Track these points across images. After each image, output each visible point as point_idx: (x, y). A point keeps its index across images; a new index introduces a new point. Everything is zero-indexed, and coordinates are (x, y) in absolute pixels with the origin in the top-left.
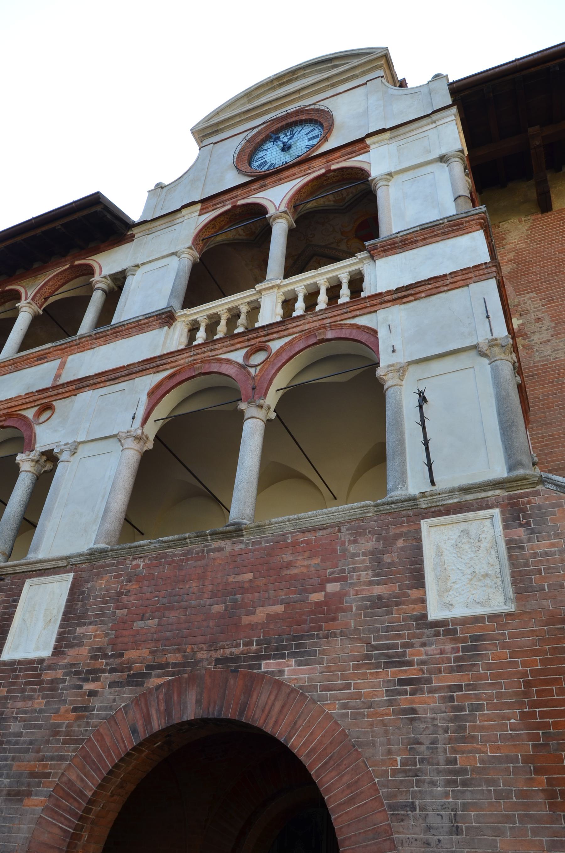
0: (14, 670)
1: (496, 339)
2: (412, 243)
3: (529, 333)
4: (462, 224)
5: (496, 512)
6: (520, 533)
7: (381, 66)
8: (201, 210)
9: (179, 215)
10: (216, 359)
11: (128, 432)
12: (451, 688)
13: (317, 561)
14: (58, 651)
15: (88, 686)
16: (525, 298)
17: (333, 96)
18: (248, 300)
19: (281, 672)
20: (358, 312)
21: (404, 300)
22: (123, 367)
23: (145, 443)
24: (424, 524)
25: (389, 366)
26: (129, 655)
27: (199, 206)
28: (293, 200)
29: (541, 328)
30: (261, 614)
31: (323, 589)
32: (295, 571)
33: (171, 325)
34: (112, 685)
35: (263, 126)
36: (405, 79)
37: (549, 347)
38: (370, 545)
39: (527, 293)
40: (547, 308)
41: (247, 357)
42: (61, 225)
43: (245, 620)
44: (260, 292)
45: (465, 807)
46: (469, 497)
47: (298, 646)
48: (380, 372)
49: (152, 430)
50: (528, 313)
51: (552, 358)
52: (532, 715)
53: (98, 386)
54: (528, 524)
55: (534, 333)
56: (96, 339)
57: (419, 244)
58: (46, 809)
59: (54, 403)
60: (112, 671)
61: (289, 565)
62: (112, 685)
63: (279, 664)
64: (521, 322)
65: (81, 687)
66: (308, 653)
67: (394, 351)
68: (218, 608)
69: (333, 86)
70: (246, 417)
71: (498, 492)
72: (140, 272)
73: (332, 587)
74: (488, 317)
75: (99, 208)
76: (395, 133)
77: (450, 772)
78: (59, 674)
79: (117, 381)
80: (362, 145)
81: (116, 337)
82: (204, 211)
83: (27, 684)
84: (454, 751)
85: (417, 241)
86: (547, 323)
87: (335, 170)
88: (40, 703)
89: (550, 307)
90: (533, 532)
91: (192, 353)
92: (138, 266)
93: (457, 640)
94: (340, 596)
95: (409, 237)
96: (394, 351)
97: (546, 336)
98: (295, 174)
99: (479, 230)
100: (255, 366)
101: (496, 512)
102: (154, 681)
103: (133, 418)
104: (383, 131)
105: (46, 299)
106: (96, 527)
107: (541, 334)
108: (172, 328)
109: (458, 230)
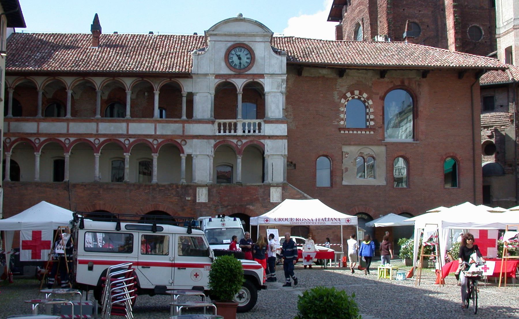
5: (281, 188)
6: (284, 192)
10: (230, 141)
13: (254, 191)
14: (209, 201)
24: (271, 188)
30: (246, 199)
38: (263, 190)
43: (243, 199)
68: (239, 197)
73: (257, 196)
78: (210, 205)
88: (208, 210)
100: (239, 146)
101: (281, 188)
102: (229, 207)
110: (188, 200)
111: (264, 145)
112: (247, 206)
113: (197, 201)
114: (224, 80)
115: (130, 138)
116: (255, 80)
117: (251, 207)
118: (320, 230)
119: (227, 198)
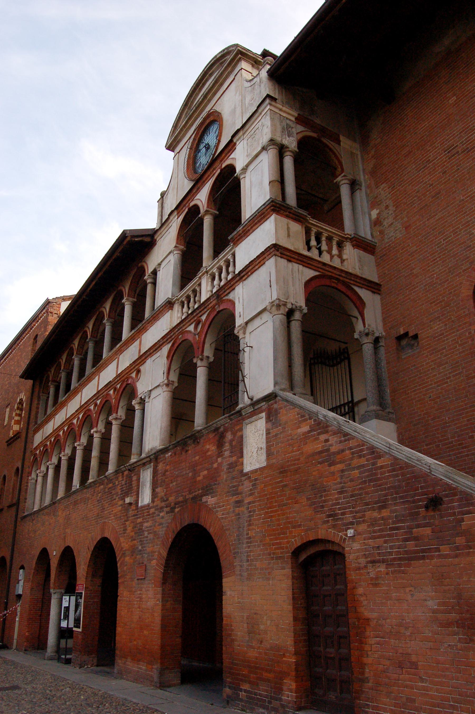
0: (143, 510)
1: (273, 302)
2: (247, 232)
3: (382, 220)
4: (264, 213)
5: (263, 414)
6: (270, 425)
7: (240, 58)
8: (178, 214)
9: (170, 221)
11: (163, 382)
12: (249, 503)
14: (153, 501)
15: (161, 514)
16: (380, 190)
17: (216, 102)
18: (198, 283)
19: (207, 501)
20: (228, 291)
21: (244, 278)
22: (156, 343)
23: (173, 385)
25: (239, 326)
26: (170, 499)
27: (175, 213)
28: (211, 197)
29: (388, 213)
31: (217, 461)
32: (209, 453)
33: (173, 307)
34: (167, 513)
35: (194, 135)
36: (264, 50)
37: (392, 229)
39: (381, 184)
40: (392, 195)
41: (196, 328)
42: (120, 252)
43: (199, 478)
44: (200, 278)
45: (251, 551)
46: (256, 408)
47: (212, 489)
48: (236, 332)
49: (174, 377)
50: (382, 202)
51: (393, 238)
52: (267, 513)
53: (153, 354)
54: (272, 420)
55: (384, 219)
56: (148, 323)
57: (251, 231)
58: (157, 565)
59: (140, 367)
60: (167, 507)
61: (208, 450)
62: (167, 513)
63: (206, 498)
64: (378, 211)
65: (159, 515)
66: (214, 492)
67: (240, 316)
68: (190, 474)
69: (222, 85)
70: (198, 366)
71: (264, 403)
72: (162, 266)
74: (271, 287)
75: (128, 239)
76: (245, 129)
77: (247, 538)
79: (157, 351)
80: (232, 144)
81: (155, 320)
82: (179, 215)
83: (147, 515)
84: (249, 530)
85: (249, 230)
86: (392, 208)
87: (225, 168)
89: (393, 194)
90: (273, 424)
91: (177, 329)
92: (160, 265)
93: (251, 481)
94: (222, 463)
95: (244, 228)
96: (240, 316)
97: (390, 220)
98: (209, 176)
99: (272, 214)
101: (263, 414)
102: (177, 510)
103: (164, 374)
104: (238, 131)
105: (135, 292)
106: (159, 438)
107: (388, 219)
108: (174, 309)
109: (264, 217)
110: (130, 504)
111: (233, 303)
112: (204, 499)
113: (140, 504)
114: (187, 210)
115: (97, 399)
116: (223, 166)
117: (210, 500)
118: (382, 568)
119: (174, 483)
